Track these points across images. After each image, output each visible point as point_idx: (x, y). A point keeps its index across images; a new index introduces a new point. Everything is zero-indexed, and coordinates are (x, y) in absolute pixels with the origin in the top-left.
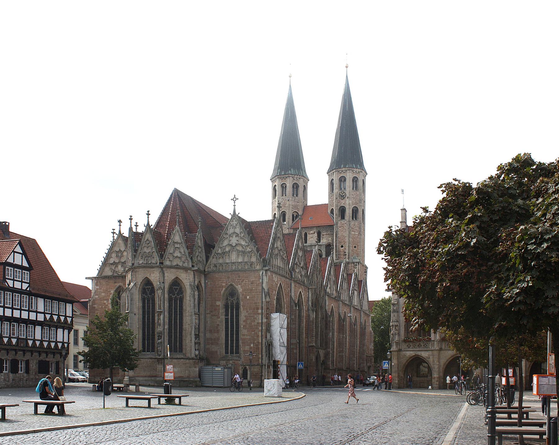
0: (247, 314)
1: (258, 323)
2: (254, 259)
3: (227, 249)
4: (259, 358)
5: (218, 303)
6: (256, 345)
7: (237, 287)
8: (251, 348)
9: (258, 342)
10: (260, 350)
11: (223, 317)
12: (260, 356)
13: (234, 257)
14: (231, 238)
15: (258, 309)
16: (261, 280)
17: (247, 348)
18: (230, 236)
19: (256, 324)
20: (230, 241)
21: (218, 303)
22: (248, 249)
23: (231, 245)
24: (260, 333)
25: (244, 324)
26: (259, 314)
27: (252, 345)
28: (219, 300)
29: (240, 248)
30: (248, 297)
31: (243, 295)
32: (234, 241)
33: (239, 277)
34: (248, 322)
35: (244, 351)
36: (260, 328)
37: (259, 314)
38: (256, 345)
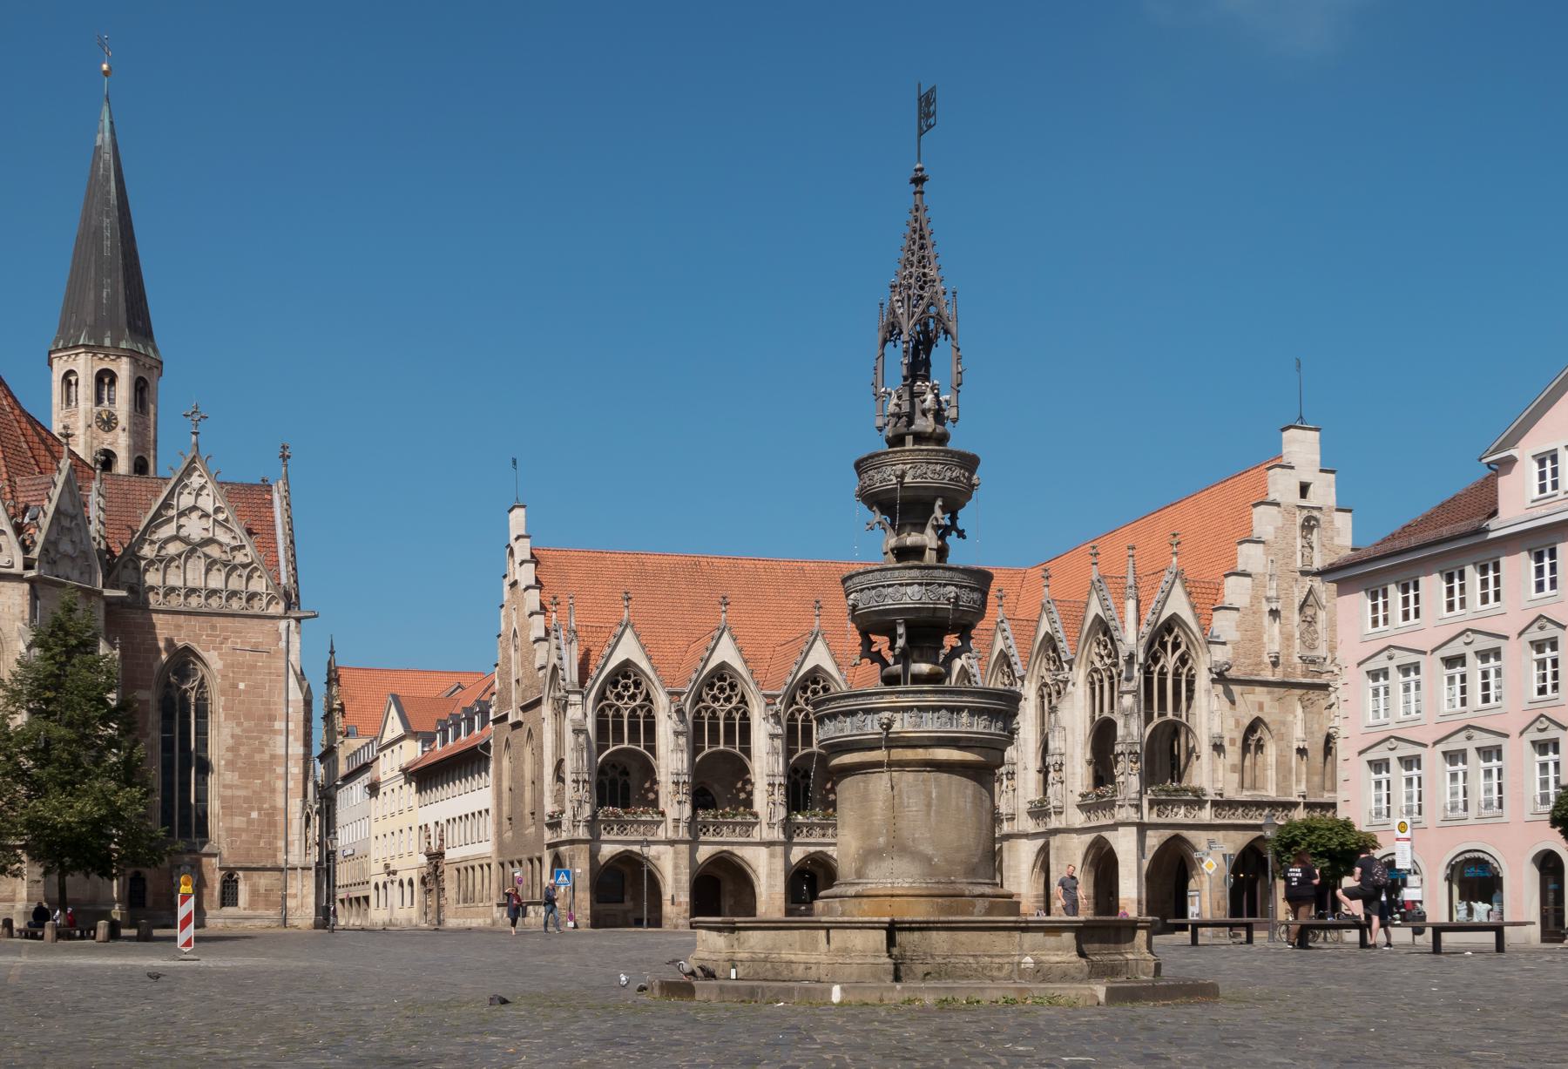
0: (238, 731)
1: (273, 757)
2: (259, 585)
3: (172, 549)
4: (276, 849)
5: (143, 695)
6: (268, 815)
7: (204, 655)
8: (250, 822)
9: (274, 808)
10: (281, 828)
11: (156, 735)
12: (281, 844)
13: (195, 574)
14: (183, 521)
15: (272, 718)
16: (283, 644)
17: (239, 822)
18: (181, 514)
19: (266, 757)
20: (180, 527)
21: (143, 695)
22: (240, 558)
23: (185, 540)
24: (280, 784)
25: (229, 755)
26: (275, 732)
27: (254, 815)
28: (148, 688)
29: (214, 551)
30: (242, 686)
31: (224, 677)
32: (195, 528)
33: (213, 627)
34: (243, 751)
35: (231, 831)
36: (280, 770)
37: (275, 732)
38: (268, 815)
